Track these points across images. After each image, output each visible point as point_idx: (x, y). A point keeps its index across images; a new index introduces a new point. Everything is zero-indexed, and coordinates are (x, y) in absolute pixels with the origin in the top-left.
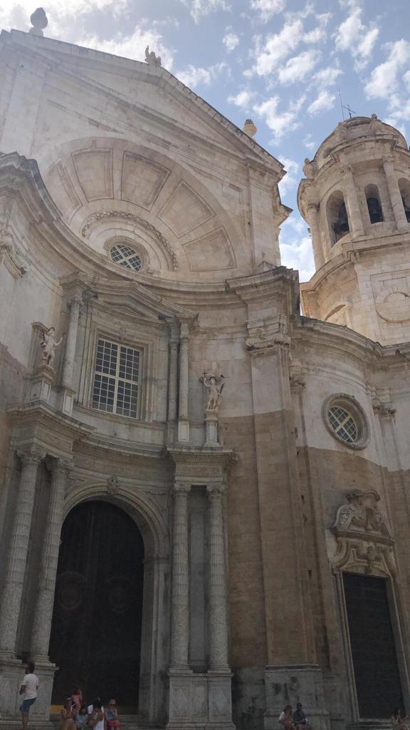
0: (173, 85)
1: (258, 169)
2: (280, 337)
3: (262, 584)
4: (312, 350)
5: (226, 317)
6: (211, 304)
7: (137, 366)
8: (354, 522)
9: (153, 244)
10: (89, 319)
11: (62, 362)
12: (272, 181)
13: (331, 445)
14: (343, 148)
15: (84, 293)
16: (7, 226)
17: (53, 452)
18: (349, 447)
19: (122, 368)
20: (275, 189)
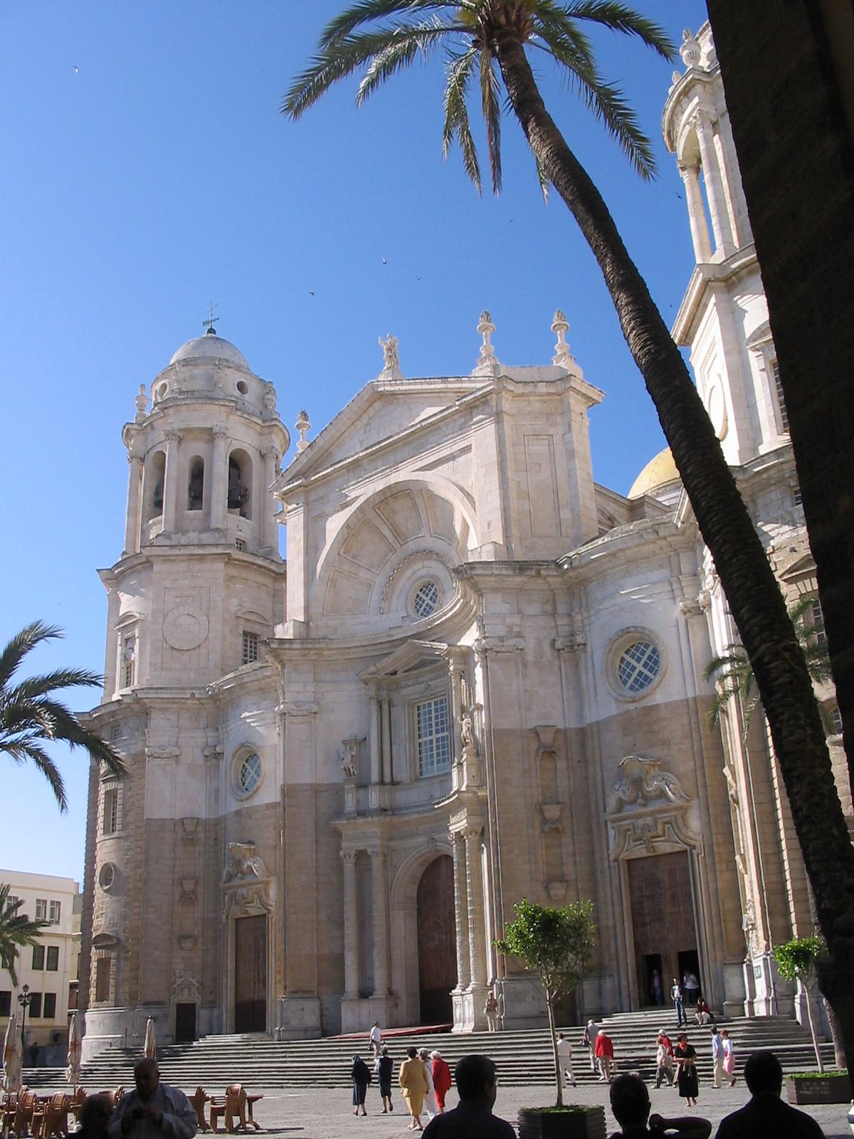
1: (477, 403)
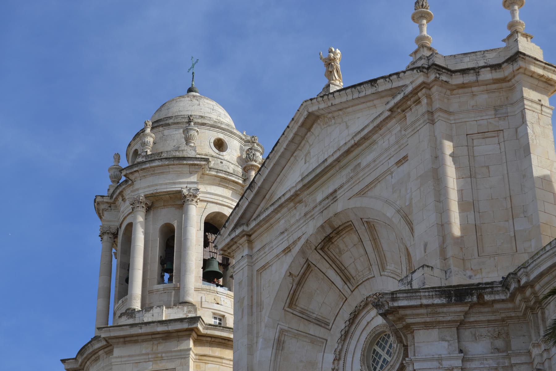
1: (409, 103)
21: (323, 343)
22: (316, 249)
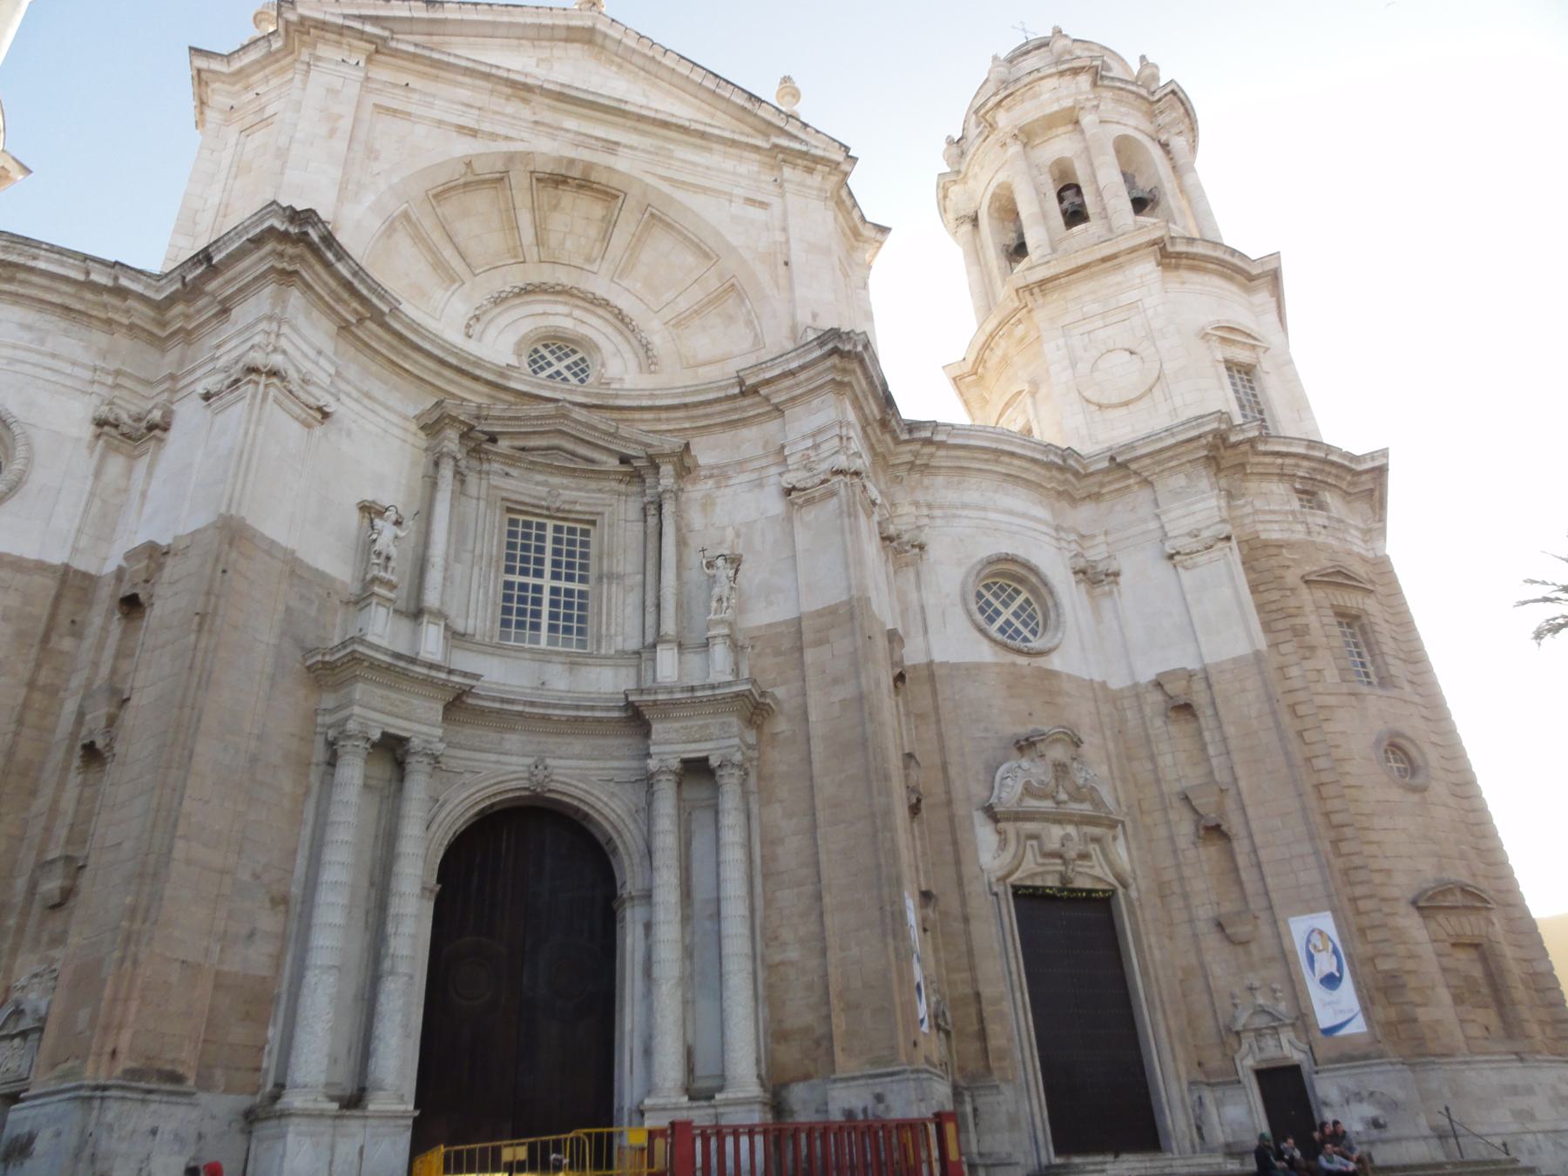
0: (618, 36)
1: (799, 161)
2: (842, 462)
3: (822, 924)
4: (940, 480)
5: (751, 440)
6: (718, 420)
7: (584, 555)
8: (1028, 791)
9: (609, 330)
10: (484, 483)
11: (421, 566)
12: (834, 179)
13: (984, 653)
14: (1001, 101)
15: (463, 436)
16: (278, 335)
17: (393, 726)
18: (1019, 652)
19: (556, 564)
20: (844, 193)
21: (453, 281)
22: (532, 172)
